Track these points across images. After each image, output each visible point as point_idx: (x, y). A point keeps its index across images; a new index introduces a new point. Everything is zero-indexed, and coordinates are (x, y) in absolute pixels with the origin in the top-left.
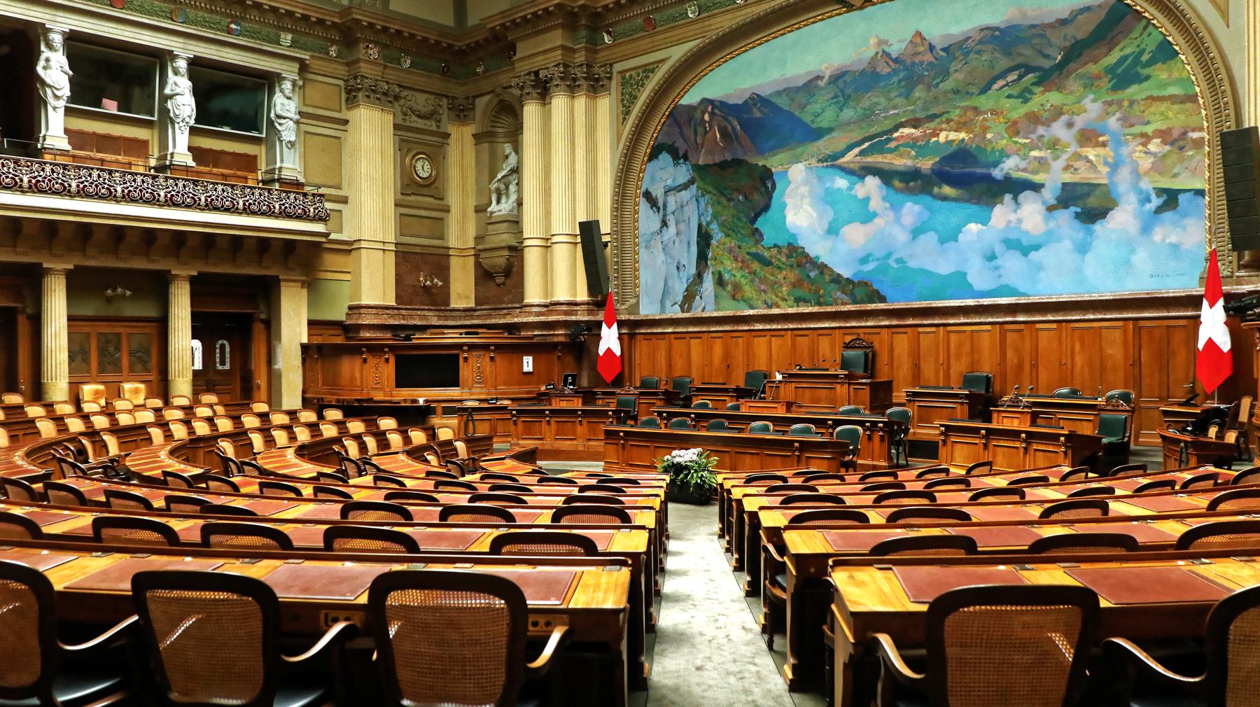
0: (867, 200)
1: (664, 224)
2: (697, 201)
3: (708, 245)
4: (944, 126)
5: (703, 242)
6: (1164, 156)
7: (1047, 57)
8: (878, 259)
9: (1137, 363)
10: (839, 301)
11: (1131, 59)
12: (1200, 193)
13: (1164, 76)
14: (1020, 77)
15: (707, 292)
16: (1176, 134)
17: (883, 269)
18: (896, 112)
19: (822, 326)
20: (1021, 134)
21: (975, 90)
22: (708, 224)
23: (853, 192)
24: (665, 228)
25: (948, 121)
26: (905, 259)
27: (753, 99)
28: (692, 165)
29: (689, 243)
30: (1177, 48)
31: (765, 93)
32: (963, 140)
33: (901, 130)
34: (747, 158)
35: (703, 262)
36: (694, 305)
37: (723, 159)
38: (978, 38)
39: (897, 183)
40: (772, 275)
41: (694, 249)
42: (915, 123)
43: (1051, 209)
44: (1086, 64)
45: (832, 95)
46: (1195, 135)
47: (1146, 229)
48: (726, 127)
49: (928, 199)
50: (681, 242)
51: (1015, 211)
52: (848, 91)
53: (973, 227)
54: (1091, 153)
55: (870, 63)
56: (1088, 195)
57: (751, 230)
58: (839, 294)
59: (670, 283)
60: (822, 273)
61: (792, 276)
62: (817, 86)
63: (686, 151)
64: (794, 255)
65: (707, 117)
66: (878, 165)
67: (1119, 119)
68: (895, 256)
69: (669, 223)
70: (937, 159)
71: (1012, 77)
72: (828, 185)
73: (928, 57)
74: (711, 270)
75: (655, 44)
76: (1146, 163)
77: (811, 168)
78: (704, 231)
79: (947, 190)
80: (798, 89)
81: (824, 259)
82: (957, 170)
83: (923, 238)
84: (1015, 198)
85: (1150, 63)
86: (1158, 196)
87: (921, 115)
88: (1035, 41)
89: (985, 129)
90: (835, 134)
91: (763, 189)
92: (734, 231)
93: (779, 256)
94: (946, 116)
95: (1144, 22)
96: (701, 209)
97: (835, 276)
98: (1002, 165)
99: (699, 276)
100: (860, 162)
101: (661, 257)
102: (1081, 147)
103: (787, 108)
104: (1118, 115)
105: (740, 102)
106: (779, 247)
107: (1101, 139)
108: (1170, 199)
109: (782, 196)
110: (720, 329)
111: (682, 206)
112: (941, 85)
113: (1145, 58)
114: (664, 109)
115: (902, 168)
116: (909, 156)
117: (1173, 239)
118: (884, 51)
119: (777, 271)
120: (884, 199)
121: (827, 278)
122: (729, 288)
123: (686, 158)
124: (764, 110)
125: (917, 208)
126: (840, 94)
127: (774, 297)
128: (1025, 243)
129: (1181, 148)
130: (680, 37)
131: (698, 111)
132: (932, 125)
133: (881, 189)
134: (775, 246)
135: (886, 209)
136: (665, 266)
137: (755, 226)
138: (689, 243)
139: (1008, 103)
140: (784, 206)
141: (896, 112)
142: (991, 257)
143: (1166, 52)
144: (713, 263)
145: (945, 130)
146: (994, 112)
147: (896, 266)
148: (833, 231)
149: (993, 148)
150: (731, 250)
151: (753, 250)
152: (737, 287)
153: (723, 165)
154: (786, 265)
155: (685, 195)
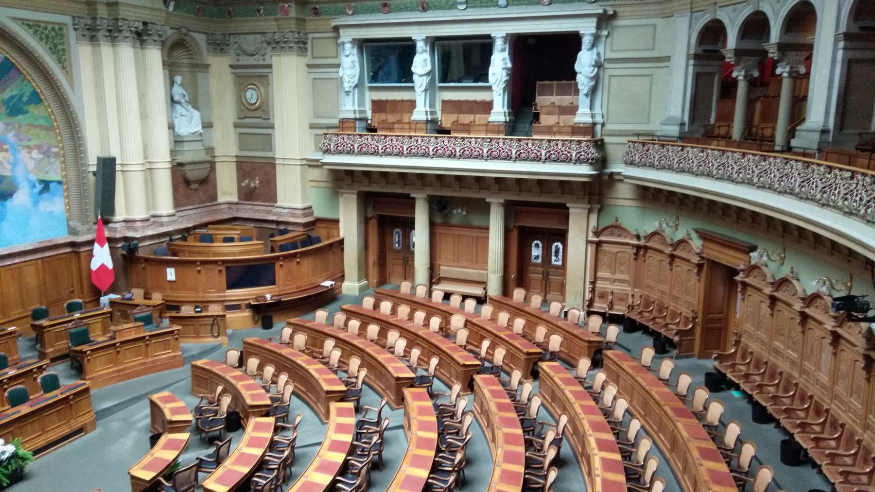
9: (44, 283)
11: (17, 97)
12: (60, 183)
13: (36, 112)
16: (45, 149)
30: (43, 97)
46: (55, 150)
47: (36, 203)
67: (14, 135)
76: (31, 164)
85: (28, 103)
95: (22, 77)
104: (13, 133)
107: (5, 147)
108: (46, 185)
113: (25, 99)
117: (49, 209)
129: (48, 157)
143: (36, 99)
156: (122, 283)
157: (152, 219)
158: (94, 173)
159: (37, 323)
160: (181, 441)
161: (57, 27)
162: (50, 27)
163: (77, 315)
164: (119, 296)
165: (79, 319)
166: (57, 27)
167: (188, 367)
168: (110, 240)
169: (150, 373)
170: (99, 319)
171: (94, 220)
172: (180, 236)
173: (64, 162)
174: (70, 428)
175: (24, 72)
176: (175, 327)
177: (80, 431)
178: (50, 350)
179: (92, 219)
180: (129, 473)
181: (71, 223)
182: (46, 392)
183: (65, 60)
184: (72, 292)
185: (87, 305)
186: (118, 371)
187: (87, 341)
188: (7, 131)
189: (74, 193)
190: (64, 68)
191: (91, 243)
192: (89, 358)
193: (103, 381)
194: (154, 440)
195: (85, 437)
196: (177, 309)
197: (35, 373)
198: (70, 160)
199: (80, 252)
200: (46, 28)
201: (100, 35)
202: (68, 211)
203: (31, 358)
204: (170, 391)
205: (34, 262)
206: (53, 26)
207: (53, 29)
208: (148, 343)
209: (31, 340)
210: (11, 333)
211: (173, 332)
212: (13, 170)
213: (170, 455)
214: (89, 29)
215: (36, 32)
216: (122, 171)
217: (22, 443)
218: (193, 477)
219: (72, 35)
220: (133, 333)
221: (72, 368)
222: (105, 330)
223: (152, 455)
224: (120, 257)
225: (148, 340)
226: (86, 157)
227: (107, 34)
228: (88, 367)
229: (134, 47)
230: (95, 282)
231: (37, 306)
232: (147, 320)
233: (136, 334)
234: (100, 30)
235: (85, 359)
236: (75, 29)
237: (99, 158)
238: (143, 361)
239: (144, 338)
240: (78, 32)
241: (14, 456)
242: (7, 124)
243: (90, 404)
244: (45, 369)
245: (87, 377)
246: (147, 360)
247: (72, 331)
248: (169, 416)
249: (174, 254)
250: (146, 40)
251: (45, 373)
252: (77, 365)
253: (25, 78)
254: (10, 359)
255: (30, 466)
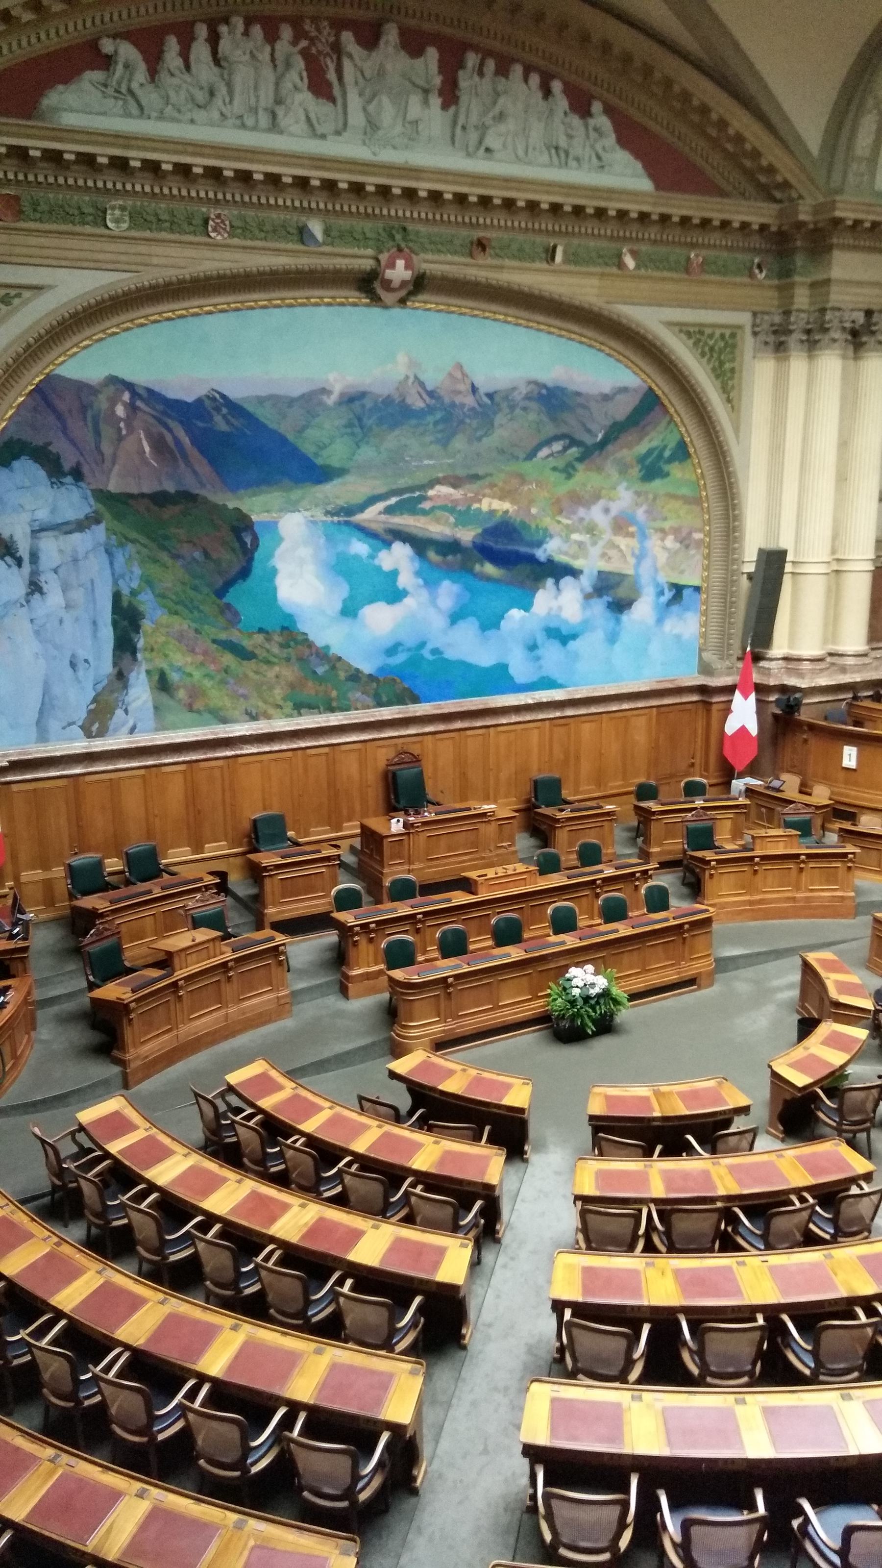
0: (395, 573)
1: (35, 587)
2: (109, 552)
3: (137, 628)
4: (487, 491)
5: (126, 623)
6: (676, 552)
7: (589, 431)
8: (409, 650)
10: (359, 705)
12: (697, 589)
14: (565, 449)
15: (138, 703)
16: (684, 533)
17: (415, 661)
18: (431, 462)
19: (348, 740)
20: (564, 513)
21: (522, 456)
22: (134, 593)
23: (376, 562)
24: (37, 596)
25: (492, 486)
26: (441, 649)
27: (214, 399)
28: (92, 491)
29: (95, 623)
30: (692, 450)
31: (234, 394)
32: (507, 512)
33: (438, 488)
34: (203, 492)
35: (128, 656)
36: (112, 724)
37: (157, 488)
38: (524, 392)
39: (432, 555)
40: (257, 673)
41: (107, 634)
42: (455, 482)
43: (587, 597)
44: (622, 448)
45: (344, 422)
46: (698, 536)
47: (660, 621)
48: (161, 437)
49: (470, 579)
50: (77, 619)
51: (556, 598)
52: (369, 422)
53: (516, 614)
54: (623, 542)
55: (398, 389)
56: (618, 584)
57: (218, 605)
58: (358, 694)
59: (57, 690)
60: (333, 668)
61: (289, 673)
62: (321, 403)
63: (78, 464)
64: (292, 643)
65: (120, 411)
66: (407, 530)
68: (430, 646)
69: (45, 588)
70: (479, 531)
71: (557, 446)
72: (341, 548)
73: (469, 401)
74: (144, 667)
75: (18, 250)
76: (662, 557)
77: (314, 523)
78: (125, 604)
79: (490, 569)
80: (291, 402)
81: (336, 650)
82: (501, 546)
83: (462, 625)
84: (557, 583)
85: (670, 460)
86: (670, 590)
87: (461, 472)
88: (580, 411)
89: (531, 502)
90: (349, 478)
91: (237, 545)
92: (186, 606)
93: (267, 646)
94: (488, 479)
95: (668, 418)
96: (117, 565)
97: (353, 672)
98: (545, 546)
99: (121, 677)
100: (384, 523)
101: (29, 647)
102: (615, 535)
103: (272, 426)
104: (644, 508)
105: (190, 399)
106: (267, 633)
108: (678, 590)
109: (271, 556)
110: (181, 759)
111: (75, 560)
112: (485, 440)
113: (667, 454)
114: (34, 378)
115: (438, 537)
116: (446, 523)
118: (416, 377)
119: (265, 667)
120: (418, 574)
121: (342, 675)
122: (182, 694)
123: (77, 474)
124: (229, 417)
125: (456, 588)
126: (356, 422)
127: (260, 704)
128: (564, 632)
129: (687, 547)
130: (82, 255)
131: (102, 397)
132: (475, 486)
133: (412, 560)
134: (261, 630)
135: (419, 586)
136: (42, 661)
137: (225, 600)
138: (95, 623)
139: (554, 477)
140: (274, 572)
141: (431, 462)
142: (533, 647)
143: (682, 452)
144: (148, 655)
145: (489, 496)
146: (539, 484)
147: (430, 657)
148: (349, 611)
149: (537, 526)
150: (182, 635)
151: (223, 636)
152: (195, 693)
153: (160, 499)
154: (280, 659)
155: (80, 541)
156: (766, 763)
157: (829, 659)
158: (750, 577)
159: (644, 804)
160: (855, 1040)
161: (728, 333)
162: (718, 332)
163: (699, 803)
164: (760, 783)
165: (702, 808)
166: (728, 333)
167: (868, 919)
168: (760, 689)
169: (799, 917)
170: (730, 814)
171: (739, 653)
172: (870, 693)
173: (708, 557)
174: (679, 973)
175: (672, 410)
176: (849, 849)
177: (691, 982)
178: (655, 850)
179: (737, 652)
180: (770, 1067)
181: (707, 656)
182: (650, 911)
183: (733, 387)
184: (693, 765)
185: (714, 789)
186: (751, 903)
187: (710, 845)
188: (637, 504)
189: (715, 608)
190: (729, 400)
191: (730, 690)
192: (713, 872)
193: (728, 912)
194: (807, 1027)
195: (698, 993)
196: (852, 817)
197: (638, 879)
198: (717, 553)
199: (711, 703)
200: (711, 336)
201: (793, 340)
202: (704, 636)
203: (629, 856)
204: (835, 953)
205: (647, 711)
206: (723, 331)
207: (722, 336)
208: (802, 865)
209: (629, 830)
210: (608, 814)
211: (845, 855)
212: (638, 565)
213: (837, 1058)
214: (775, 332)
215: (696, 344)
216: (792, 573)
217: (617, 978)
218: (869, 1106)
219: (748, 343)
220: (781, 844)
221: (684, 883)
222: (737, 834)
223: (806, 1048)
224: (770, 719)
225: (803, 862)
226: (741, 547)
227: (804, 338)
228: (709, 886)
229: (844, 357)
230: (728, 753)
231: (642, 780)
232: (804, 829)
233: (786, 848)
234: (791, 332)
235: (707, 873)
236: (755, 334)
237: (761, 552)
238: (789, 895)
239: (797, 856)
240: (758, 338)
241: (605, 994)
242: (638, 494)
243: (710, 945)
244: (650, 877)
245: (706, 902)
246: (799, 895)
247: (691, 825)
248: (833, 993)
249: (857, 723)
250: (865, 343)
251: (651, 883)
252: (692, 880)
253: (672, 419)
254: (604, 851)
255: (625, 1014)
